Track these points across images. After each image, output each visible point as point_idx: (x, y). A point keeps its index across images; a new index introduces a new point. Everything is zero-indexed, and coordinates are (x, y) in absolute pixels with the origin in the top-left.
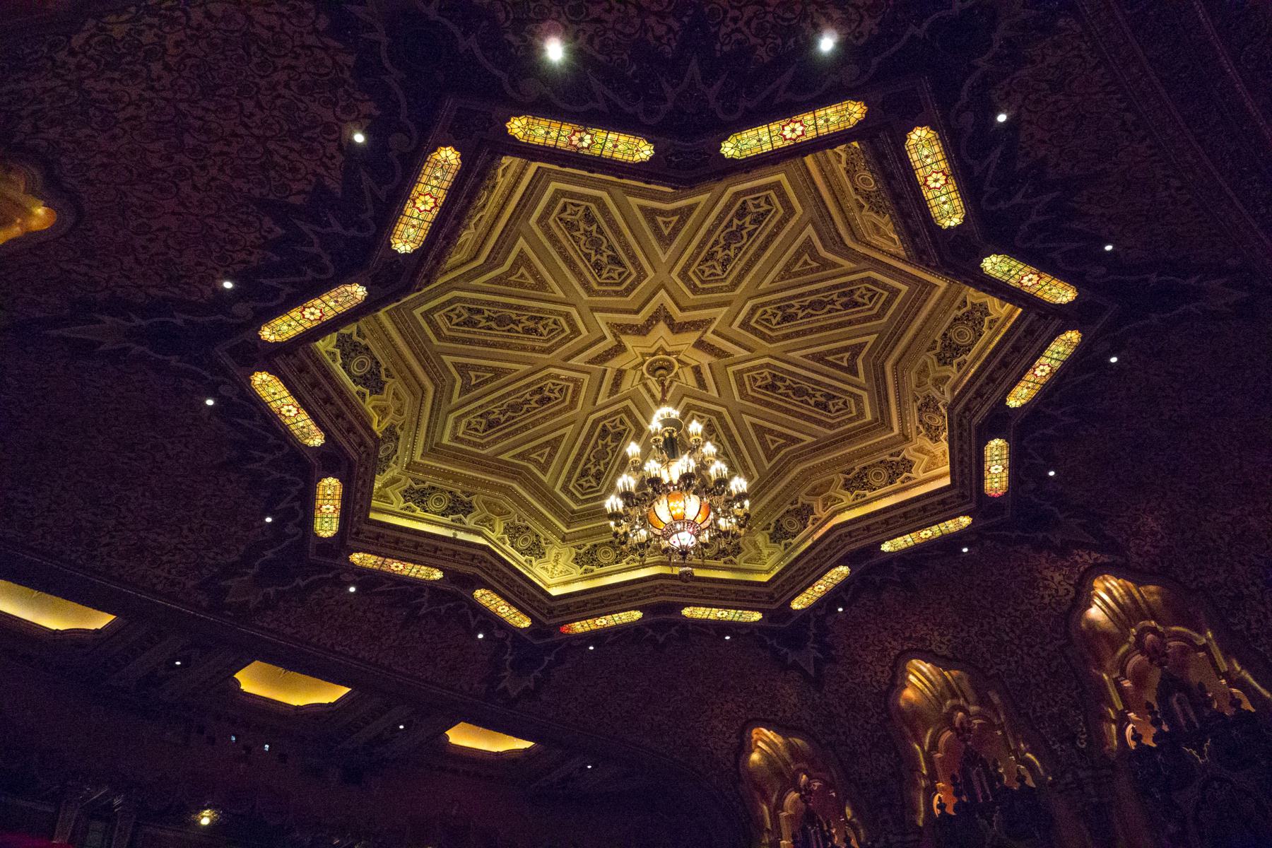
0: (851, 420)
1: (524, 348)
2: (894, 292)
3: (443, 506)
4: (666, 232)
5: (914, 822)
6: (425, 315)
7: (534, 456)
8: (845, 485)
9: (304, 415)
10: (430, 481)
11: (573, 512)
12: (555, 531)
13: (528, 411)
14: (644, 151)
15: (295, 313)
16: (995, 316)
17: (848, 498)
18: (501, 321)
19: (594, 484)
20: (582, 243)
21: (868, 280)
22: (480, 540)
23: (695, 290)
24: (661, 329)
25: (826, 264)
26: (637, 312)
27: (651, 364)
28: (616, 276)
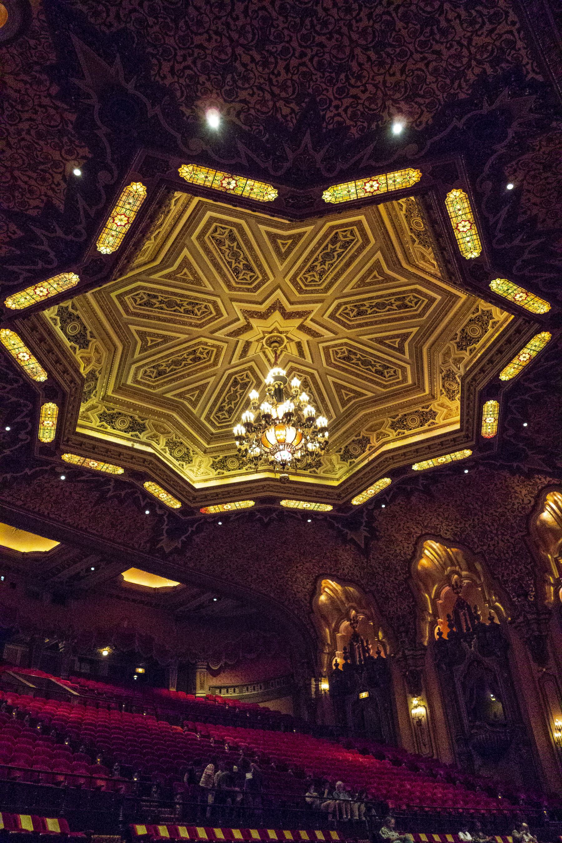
0: (398, 383)
1: (184, 323)
2: (432, 300)
3: (126, 426)
4: (283, 250)
5: (422, 643)
6: (119, 297)
7: (187, 396)
9: (34, 360)
10: (118, 409)
11: (212, 434)
12: (199, 445)
13: (185, 366)
14: (270, 194)
15: (30, 290)
16: (496, 319)
17: (393, 434)
18: (170, 304)
19: (227, 416)
20: (226, 254)
21: (416, 291)
22: (149, 450)
23: (301, 291)
24: (277, 315)
25: (388, 279)
26: (261, 303)
28: (248, 278)
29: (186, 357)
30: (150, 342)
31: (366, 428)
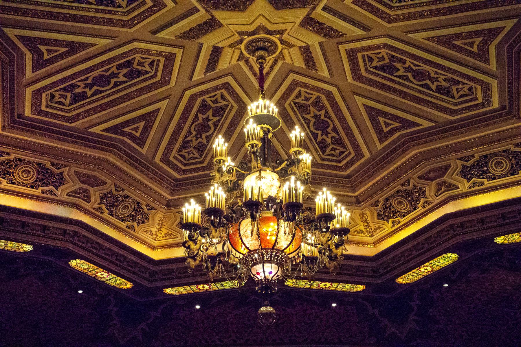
0: (476, 106)
7: (127, 130)
8: (462, 172)
11: (177, 180)
12: (158, 198)
13: (116, 85)
17: (464, 186)
19: (197, 155)
29: (116, 71)
30: (46, 54)
31: (420, 173)
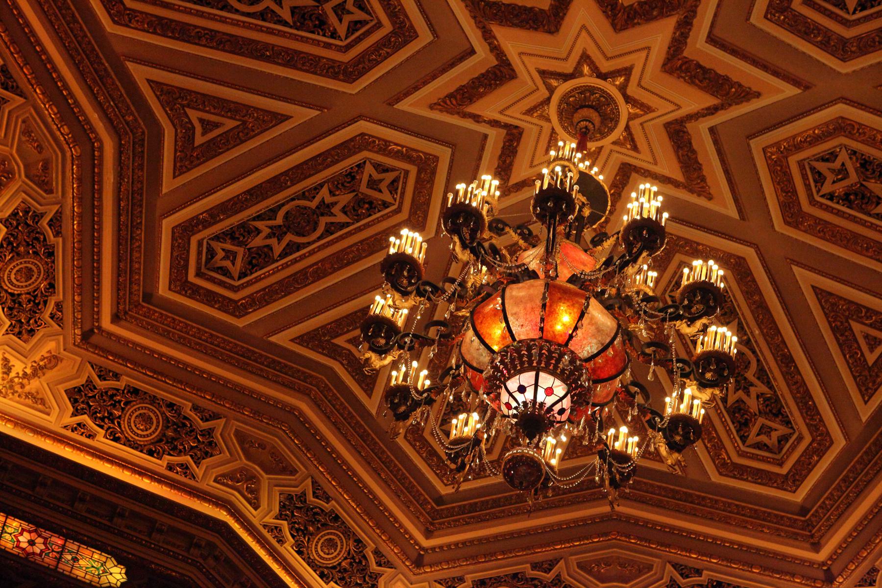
11: (440, 500)
12: (396, 534)
13: (328, 231)
27: (565, 98)
